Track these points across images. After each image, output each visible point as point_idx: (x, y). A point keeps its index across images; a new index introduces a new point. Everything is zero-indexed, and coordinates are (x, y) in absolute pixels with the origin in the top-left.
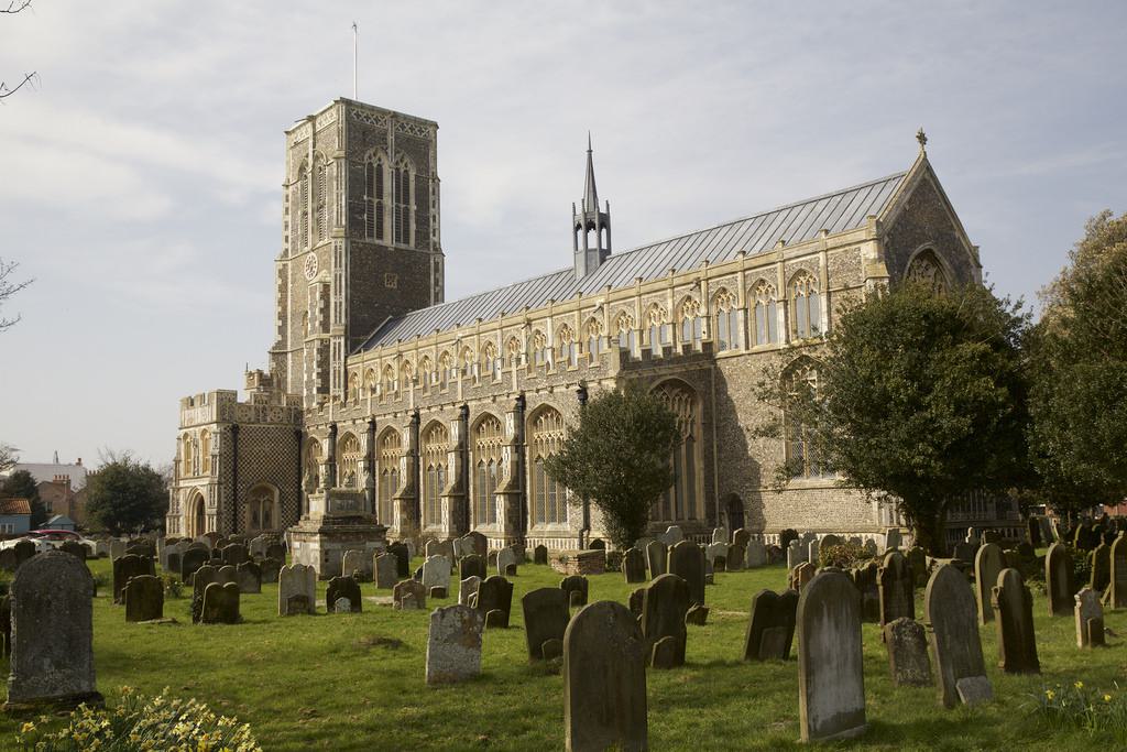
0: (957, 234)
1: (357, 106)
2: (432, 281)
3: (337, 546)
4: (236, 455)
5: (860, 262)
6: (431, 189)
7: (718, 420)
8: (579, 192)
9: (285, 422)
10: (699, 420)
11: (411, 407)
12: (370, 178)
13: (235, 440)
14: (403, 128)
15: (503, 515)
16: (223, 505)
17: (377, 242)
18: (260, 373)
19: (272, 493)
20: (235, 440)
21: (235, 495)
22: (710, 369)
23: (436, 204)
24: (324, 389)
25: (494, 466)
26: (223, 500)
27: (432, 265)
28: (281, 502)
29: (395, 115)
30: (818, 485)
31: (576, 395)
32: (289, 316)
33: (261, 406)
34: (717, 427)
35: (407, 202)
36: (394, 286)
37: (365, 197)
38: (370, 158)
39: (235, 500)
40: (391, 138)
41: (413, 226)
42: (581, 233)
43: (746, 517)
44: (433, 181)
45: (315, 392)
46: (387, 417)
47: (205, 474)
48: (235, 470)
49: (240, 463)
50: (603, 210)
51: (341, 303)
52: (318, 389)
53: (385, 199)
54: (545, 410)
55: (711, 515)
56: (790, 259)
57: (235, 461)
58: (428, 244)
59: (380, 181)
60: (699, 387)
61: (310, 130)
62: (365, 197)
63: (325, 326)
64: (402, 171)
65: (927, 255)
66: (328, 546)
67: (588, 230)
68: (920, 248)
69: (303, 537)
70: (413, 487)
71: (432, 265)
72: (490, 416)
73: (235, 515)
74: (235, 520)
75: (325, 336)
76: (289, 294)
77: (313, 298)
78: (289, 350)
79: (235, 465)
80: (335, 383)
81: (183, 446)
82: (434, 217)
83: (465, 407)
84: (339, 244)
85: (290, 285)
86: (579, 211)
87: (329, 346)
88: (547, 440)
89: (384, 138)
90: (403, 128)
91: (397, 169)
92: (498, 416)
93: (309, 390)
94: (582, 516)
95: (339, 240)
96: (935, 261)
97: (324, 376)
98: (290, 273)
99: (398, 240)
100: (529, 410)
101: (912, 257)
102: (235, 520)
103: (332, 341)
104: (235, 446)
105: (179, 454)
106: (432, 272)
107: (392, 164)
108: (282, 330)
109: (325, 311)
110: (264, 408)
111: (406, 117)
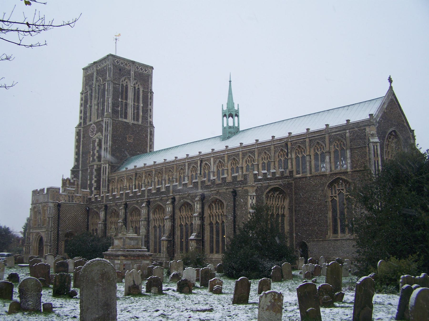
0: (405, 124)
1: (118, 58)
3: (129, 262)
4: (59, 218)
5: (365, 135)
6: (149, 97)
7: (296, 207)
13: (59, 210)
14: (138, 68)
16: (52, 241)
20: (59, 210)
22: (292, 183)
23: (151, 103)
24: (98, 188)
26: (52, 239)
27: (149, 132)
29: (133, 62)
31: (230, 193)
34: (295, 211)
35: (138, 102)
36: (131, 141)
37: (120, 100)
38: (122, 82)
40: (132, 73)
41: (141, 114)
44: (151, 93)
45: (93, 189)
49: (61, 222)
50: (236, 108)
51: (107, 148)
52: (95, 189)
53: (128, 100)
56: (332, 132)
57: (58, 221)
58: (147, 122)
61: (95, 68)
62: (120, 100)
64: (137, 88)
67: (229, 117)
69: (112, 258)
71: (149, 132)
72: (188, 204)
75: (99, 163)
76: (81, 143)
77: (94, 145)
80: (103, 185)
82: (151, 110)
83: (174, 199)
84: (107, 121)
85: (82, 139)
86: (225, 108)
87: (100, 168)
89: (129, 74)
90: (138, 68)
91: (135, 87)
92: (191, 203)
95: (107, 118)
96: (396, 136)
97: (98, 182)
99: (134, 119)
101: (388, 134)
103: (102, 166)
105: (31, 216)
107: (132, 85)
108: (77, 160)
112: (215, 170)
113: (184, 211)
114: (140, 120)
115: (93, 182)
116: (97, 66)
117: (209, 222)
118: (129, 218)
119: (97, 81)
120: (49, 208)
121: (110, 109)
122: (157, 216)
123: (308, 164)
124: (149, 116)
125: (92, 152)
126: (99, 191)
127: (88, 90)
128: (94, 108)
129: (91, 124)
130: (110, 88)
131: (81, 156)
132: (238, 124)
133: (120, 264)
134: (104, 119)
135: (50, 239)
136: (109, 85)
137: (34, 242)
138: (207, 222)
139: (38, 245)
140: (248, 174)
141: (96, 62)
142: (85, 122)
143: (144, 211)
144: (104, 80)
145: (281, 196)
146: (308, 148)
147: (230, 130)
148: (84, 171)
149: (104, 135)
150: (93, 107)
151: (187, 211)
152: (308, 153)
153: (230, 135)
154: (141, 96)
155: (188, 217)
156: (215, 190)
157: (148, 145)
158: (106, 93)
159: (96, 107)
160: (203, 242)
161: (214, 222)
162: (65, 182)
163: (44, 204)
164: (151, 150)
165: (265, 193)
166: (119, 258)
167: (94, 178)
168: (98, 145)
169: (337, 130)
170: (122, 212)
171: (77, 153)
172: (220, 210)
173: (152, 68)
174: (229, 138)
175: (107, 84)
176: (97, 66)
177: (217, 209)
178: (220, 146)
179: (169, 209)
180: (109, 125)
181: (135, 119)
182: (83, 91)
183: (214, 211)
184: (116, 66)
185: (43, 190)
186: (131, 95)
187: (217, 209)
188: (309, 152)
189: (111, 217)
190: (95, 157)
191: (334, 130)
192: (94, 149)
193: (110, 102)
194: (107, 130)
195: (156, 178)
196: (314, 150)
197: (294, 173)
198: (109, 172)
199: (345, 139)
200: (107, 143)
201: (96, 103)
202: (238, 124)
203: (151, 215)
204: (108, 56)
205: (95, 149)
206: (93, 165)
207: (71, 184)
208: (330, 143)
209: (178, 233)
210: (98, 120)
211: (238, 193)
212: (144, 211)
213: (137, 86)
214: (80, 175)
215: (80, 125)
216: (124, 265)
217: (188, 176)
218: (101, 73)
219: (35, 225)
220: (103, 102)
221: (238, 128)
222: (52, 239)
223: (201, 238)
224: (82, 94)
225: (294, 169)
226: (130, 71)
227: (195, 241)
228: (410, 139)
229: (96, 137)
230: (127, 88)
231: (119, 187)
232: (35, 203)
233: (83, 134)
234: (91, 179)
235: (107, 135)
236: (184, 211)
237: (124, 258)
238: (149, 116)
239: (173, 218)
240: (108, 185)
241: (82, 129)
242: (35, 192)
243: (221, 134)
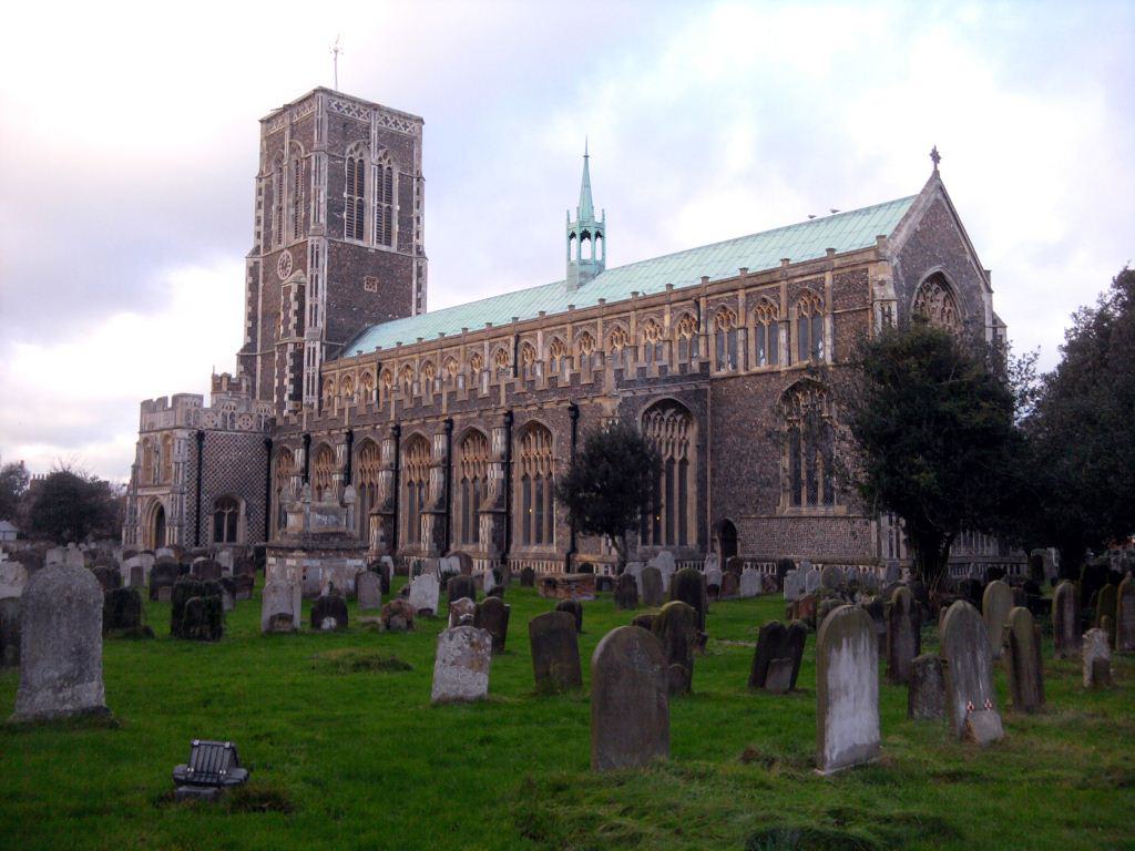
0: (969, 258)
2: (414, 286)
3: (316, 563)
4: (200, 464)
6: (415, 189)
7: (713, 443)
8: (573, 202)
9: (254, 429)
10: (692, 444)
11: (392, 417)
13: (200, 447)
14: (387, 122)
15: (486, 535)
16: (185, 516)
18: (229, 377)
19: (237, 505)
20: (200, 447)
21: (199, 506)
22: (706, 390)
24: (297, 396)
25: (479, 483)
26: (185, 510)
28: (248, 514)
29: (376, 107)
30: (814, 514)
31: (566, 411)
32: (260, 317)
33: (229, 413)
34: (712, 450)
35: (389, 200)
37: (345, 195)
38: (351, 152)
39: (198, 511)
40: (374, 132)
41: (396, 228)
42: (574, 241)
43: (739, 544)
45: (286, 398)
46: (366, 428)
47: (166, 482)
48: (199, 480)
50: (598, 219)
51: (316, 306)
52: (291, 397)
54: (535, 427)
55: (702, 540)
56: (795, 277)
57: (199, 469)
58: (411, 247)
60: (694, 407)
61: (287, 121)
62: (345, 195)
63: (300, 329)
65: (938, 278)
66: (306, 563)
67: (582, 238)
69: (281, 553)
70: (394, 503)
72: (476, 432)
73: (198, 527)
74: (198, 532)
75: (297, 339)
76: (260, 293)
77: (287, 299)
78: (259, 352)
79: (200, 474)
81: (142, 452)
82: (418, 219)
83: (450, 422)
85: (261, 284)
86: (573, 219)
88: (536, 459)
90: (387, 122)
93: (281, 397)
94: (569, 538)
95: (317, 238)
97: (297, 382)
98: (261, 270)
100: (516, 426)
101: (922, 280)
102: (198, 532)
104: (200, 454)
105: (138, 459)
106: (414, 276)
108: (251, 332)
109: (300, 313)
110: (232, 415)
111: (389, 111)
112: (546, 358)
113: (472, 449)
115: (286, 382)
116: (292, 116)
117: (522, 474)
118: (357, 464)
119: (293, 150)
120: (176, 442)
121: (322, 216)
122: (415, 460)
123: (741, 348)
124: (414, 233)
125: (282, 314)
126: (299, 403)
127: (273, 170)
128: (288, 212)
129: (282, 251)
131: (260, 322)
132: (603, 254)
133: (294, 567)
134: (310, 239)
135: (181, 512)
136: (318, 159)
137: (144, 518)
138: (517, 473)
139: (154, 525)
140: (604, 371)
141: (289, 105)
142: (267, 247)
143: (387, 449)
144: (309, 147)
145: (679, 418)
147: (584, 268)
148: (267, 357)
149: (309, 276)
150: (284, 212)
151: (477, 448)
152: (741, 324)
153: (583, 279)
154: (396, 184)
155: (478, 462)
156: (535, 404)
157: (414, 301)
158: (313, 178)
159: (292, 211)
160: (509, 519)
161: (532, 475)
162: (219, 383)
163: (165, 432)
164: (419, 310)
165: (642, 411)
166: (294, 554)
167: (287, 371)
168: (296, 299)
169: (806, 271)
170: (341, 451)
171: (252, 317)
172: (546, 449)
173: (421, 121)
174: (580, 285)
175: (313, 158)
176: (292, 116)
177: (539, 444)
178: (556, 306)
179: (439, 444)
180: (321, 253)
181: (383, 239)
182: (261, 173)
183: (534, 450)
184: (335, 116)
185: (163, 400)
186: (371, 183)
187: (539, 444)
188: (746, 320)
189: (318, 461)
190: (291, 326)
191: (800, 272)
192: (286, 308)
193: (322, 201)
194: (315, 263)
195: (423, 374)
196: (756, 315)
197: (712, 368)
198: (321, 360)
199: (823, 293)
200: (316, 293)
201: (291, 201)
202: (603, 254)
203: (403, 458)
204: (315, 91)
205: (290, 307)
206: (286, 344)
207: (234, 386)
208: (791, 301)
209: (458, 498)
210: (297, 241)
211: (581, 411)
212: (387, 449)
213: (385, 162)
214: (259, 366)
215: (256, 251)
216: (305, 569)
217: (490, 372)
218: (301, 130)
219: (148, 479)
220: (308, 201)
221: (601, 267)
222: (185, 510)
223: (504, 510)
224: (259, 179)
225: (712, 358)
226: (368, 128)
227: (491, 516)
228: (979, 290)
229: (289, 280)
232: (147, 428)
233: (264, 273)
234: (282, 376)
235: (317, 277)
236: (472, 449)
237: (304, 554)
238: (414, 233)
239: (447, 466)
241: (261, 261)
242: (148, 407)
243: (561, 275)
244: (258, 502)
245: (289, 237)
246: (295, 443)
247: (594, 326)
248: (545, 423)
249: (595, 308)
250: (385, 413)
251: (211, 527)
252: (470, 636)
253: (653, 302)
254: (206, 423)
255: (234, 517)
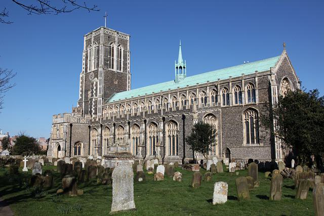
3: (121, 161)
7: (222, 126)
12: (110, 51)
17: (113, 70)
21: (70, 145)
35: (120, 58)
36: (117, 83)
40: (116, 39)
55: (220, 154)
59: (113, 52)
60: (217, 116)
68: (284, 77)
73: (70, 151)
74: (70, 153)
75: (96, 97)
77: (93, 86)
97: (96, 109)
102: (70, 153)
112: (171, 102)
114: (122, 69)
115: (92, 109)
130: (102, 48)
146: (231, 88)
148: (86, 102)
161: (171, 135)
213: (119, 47)
214: (84, 105)
230: (113, 50)
231: (109, 113)
234: (91, 108)
240: (102, 111)
244: (87, 144)
245: (93, 69)
246: (98, 127)
247: (186, 93)
248: (175, 120)
249: (186, 88)
250: (125, 118)
251: (74, 151)
252: (223, 184)
253: (203, 86)
254: (72, 121)
255: (80, 148)
